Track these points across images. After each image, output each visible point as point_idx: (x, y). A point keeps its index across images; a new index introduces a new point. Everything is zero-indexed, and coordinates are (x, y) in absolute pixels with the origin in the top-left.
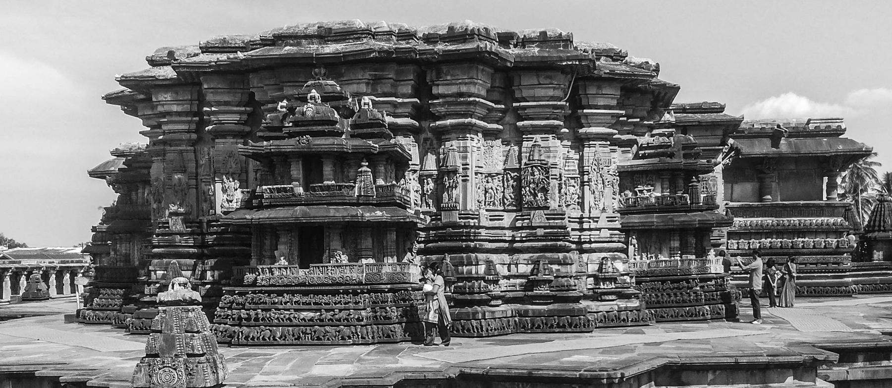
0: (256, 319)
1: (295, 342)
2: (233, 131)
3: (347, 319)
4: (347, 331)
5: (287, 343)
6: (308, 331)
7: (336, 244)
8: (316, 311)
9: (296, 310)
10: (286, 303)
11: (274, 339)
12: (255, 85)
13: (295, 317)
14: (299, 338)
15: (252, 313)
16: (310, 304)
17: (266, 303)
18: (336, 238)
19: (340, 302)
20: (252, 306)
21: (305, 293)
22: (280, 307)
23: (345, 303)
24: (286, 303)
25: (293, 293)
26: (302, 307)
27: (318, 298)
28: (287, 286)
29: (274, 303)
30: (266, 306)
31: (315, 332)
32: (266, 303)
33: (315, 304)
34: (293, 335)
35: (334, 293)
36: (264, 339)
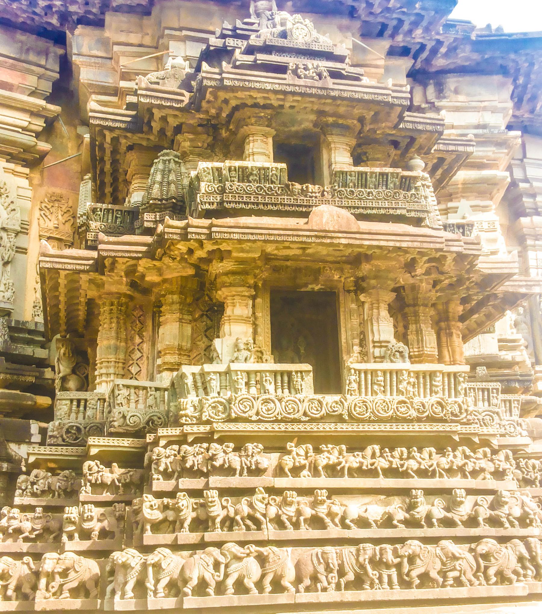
0: (202, 523)
1: (350, 596)
2: (13, 143)
3: (494, 522)
4: (507, 557)
5: (323, 598)
6: (389, 557)
7: (384, 329)
8: (389, 492)
9: (333, 492)
10: (296, 471)
11: (278, 586)
12: (85, 50)
13: (330, 514)
14: (358, 583)
15: (186, 504)
16: (372, 473)
17: (230, 471)
18: (384, 313)
19: (461, 470)
20: (186, 483)
21: (356, 444)
22: (280, 482)
23: (475, 473)
24: (296, 471)
25: (317, 442)
26: (345, 482)
27: (395, 458)
28: (284, 420)
29: (258, 471)
30: (235, 482)
31: (411, 559)
32: (230, 471)
33: (391, 472)
34: (342, 573)
35: (442, 443)
36: (241, 587)
